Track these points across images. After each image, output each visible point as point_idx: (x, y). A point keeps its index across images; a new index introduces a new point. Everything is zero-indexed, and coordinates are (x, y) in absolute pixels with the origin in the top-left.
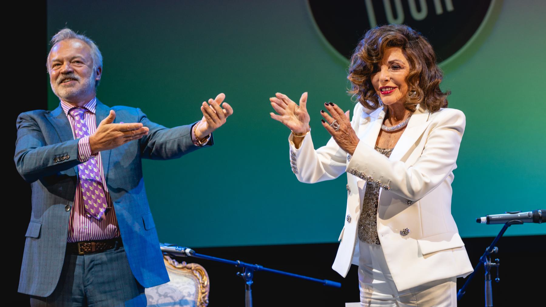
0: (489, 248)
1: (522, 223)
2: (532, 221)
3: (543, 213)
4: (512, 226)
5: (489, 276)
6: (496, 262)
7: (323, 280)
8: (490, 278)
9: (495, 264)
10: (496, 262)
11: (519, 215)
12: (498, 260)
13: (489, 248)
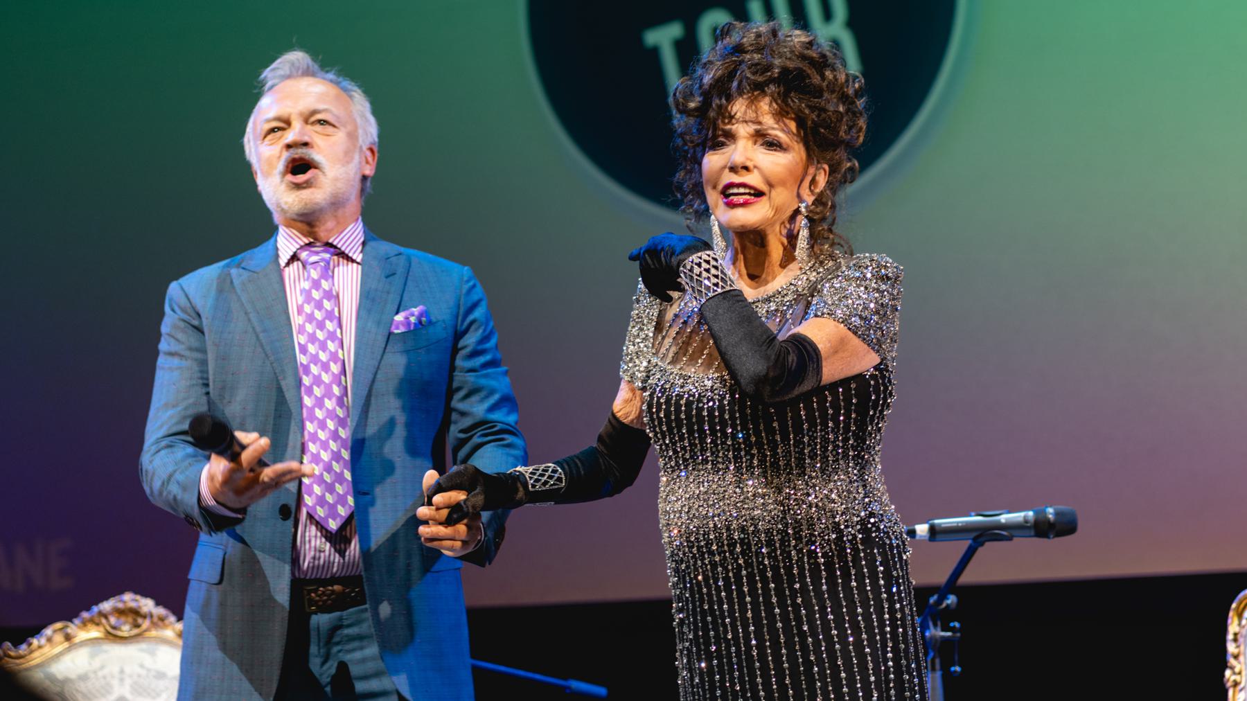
0: (935, 597)
1: (1010, 538)
2: (1033, 533)
3: (1057, 514)
4: (988, 544)
5: (937, 661)
6: (953, 629)
7: (566, 679)
8: (938, 666)
9: (949, 634)
10: (953, 629)
11: (1004, 518)
12: (957, 625)
13: (935, 597)
